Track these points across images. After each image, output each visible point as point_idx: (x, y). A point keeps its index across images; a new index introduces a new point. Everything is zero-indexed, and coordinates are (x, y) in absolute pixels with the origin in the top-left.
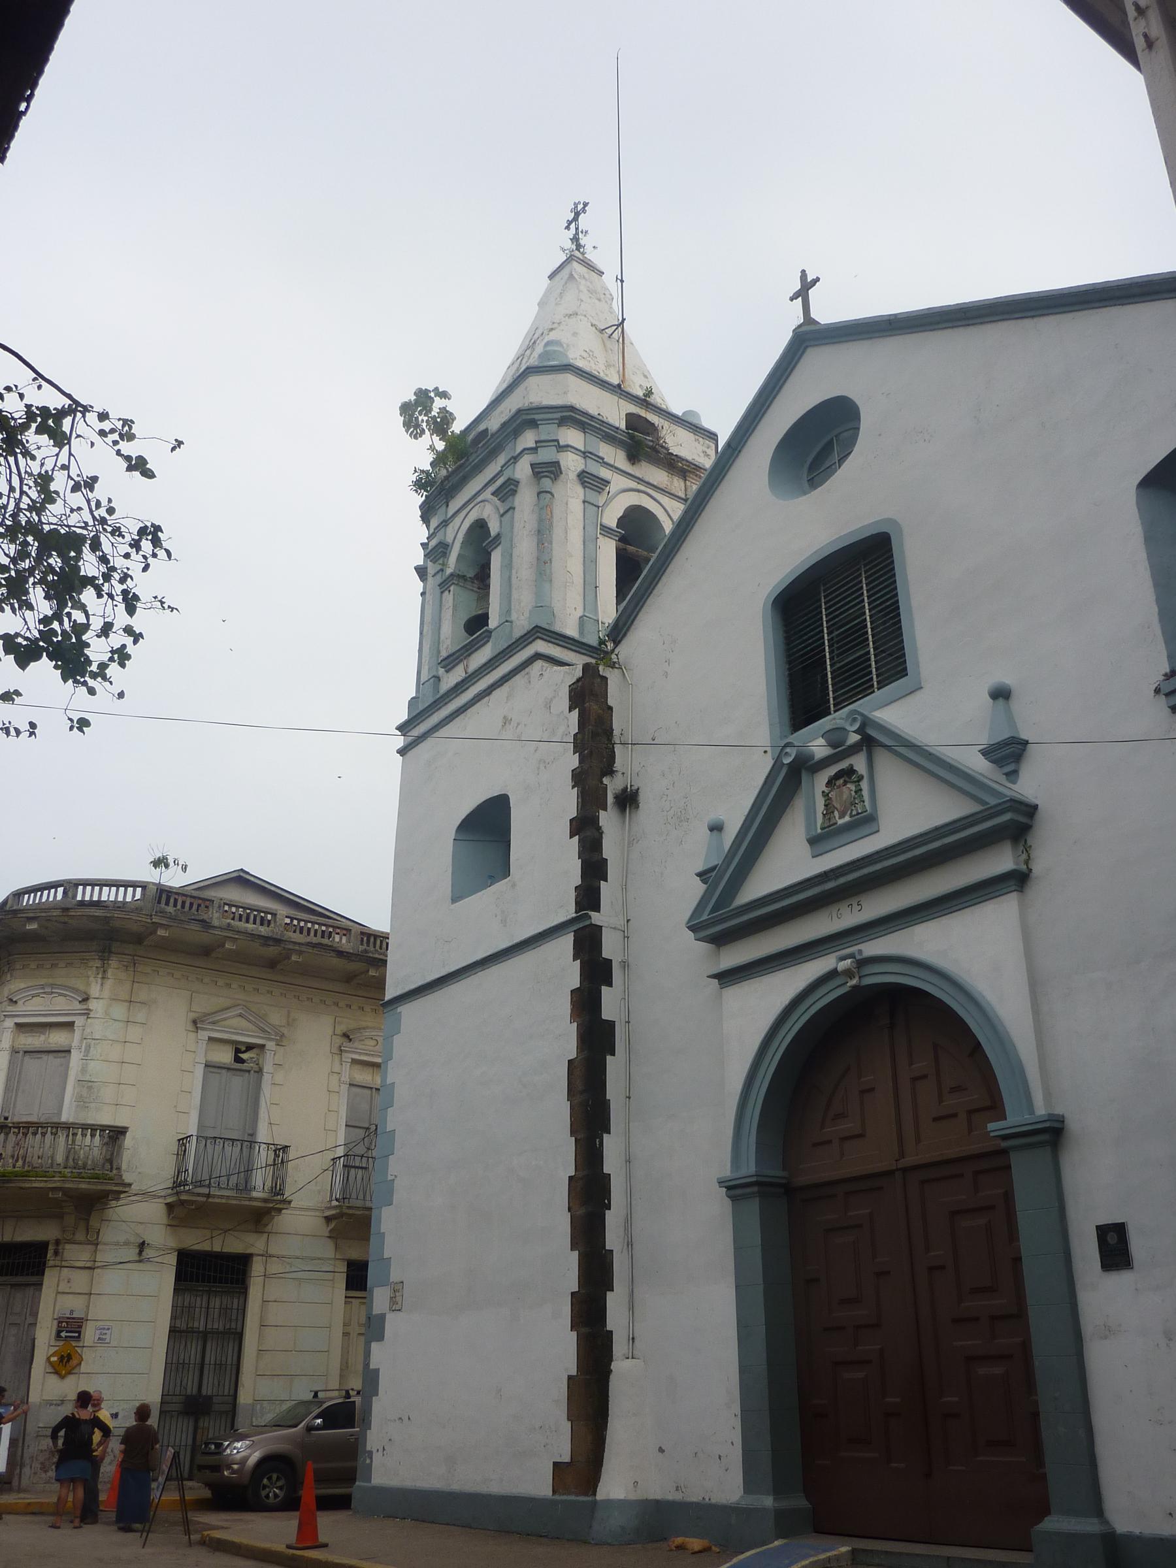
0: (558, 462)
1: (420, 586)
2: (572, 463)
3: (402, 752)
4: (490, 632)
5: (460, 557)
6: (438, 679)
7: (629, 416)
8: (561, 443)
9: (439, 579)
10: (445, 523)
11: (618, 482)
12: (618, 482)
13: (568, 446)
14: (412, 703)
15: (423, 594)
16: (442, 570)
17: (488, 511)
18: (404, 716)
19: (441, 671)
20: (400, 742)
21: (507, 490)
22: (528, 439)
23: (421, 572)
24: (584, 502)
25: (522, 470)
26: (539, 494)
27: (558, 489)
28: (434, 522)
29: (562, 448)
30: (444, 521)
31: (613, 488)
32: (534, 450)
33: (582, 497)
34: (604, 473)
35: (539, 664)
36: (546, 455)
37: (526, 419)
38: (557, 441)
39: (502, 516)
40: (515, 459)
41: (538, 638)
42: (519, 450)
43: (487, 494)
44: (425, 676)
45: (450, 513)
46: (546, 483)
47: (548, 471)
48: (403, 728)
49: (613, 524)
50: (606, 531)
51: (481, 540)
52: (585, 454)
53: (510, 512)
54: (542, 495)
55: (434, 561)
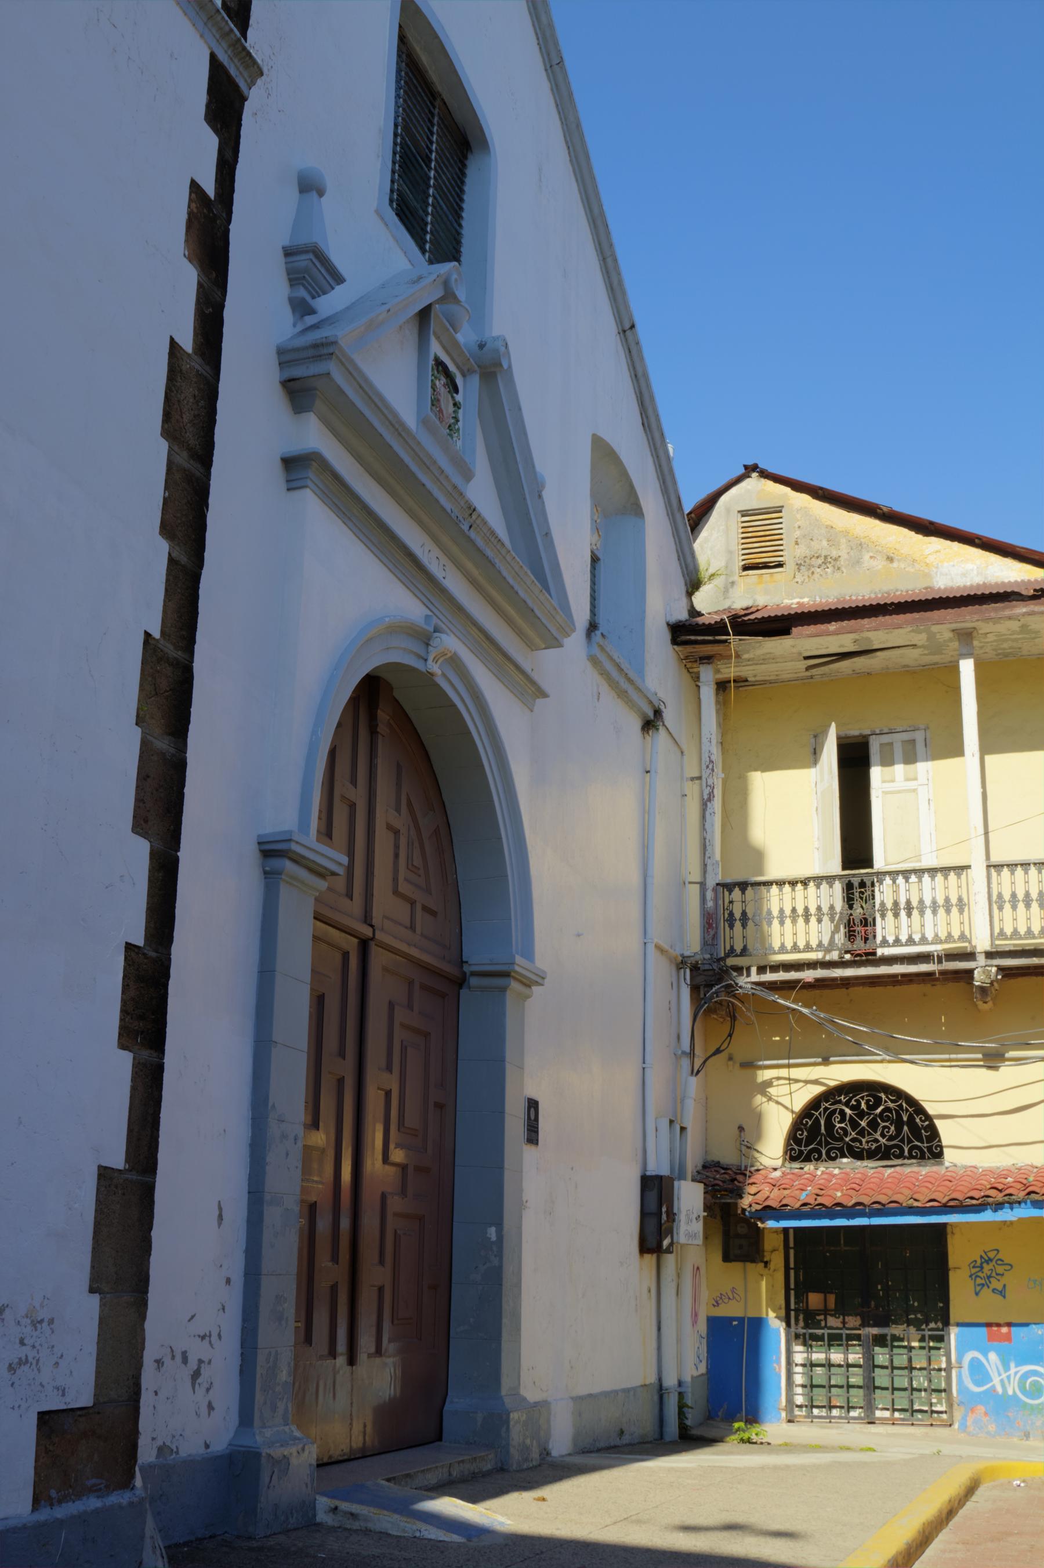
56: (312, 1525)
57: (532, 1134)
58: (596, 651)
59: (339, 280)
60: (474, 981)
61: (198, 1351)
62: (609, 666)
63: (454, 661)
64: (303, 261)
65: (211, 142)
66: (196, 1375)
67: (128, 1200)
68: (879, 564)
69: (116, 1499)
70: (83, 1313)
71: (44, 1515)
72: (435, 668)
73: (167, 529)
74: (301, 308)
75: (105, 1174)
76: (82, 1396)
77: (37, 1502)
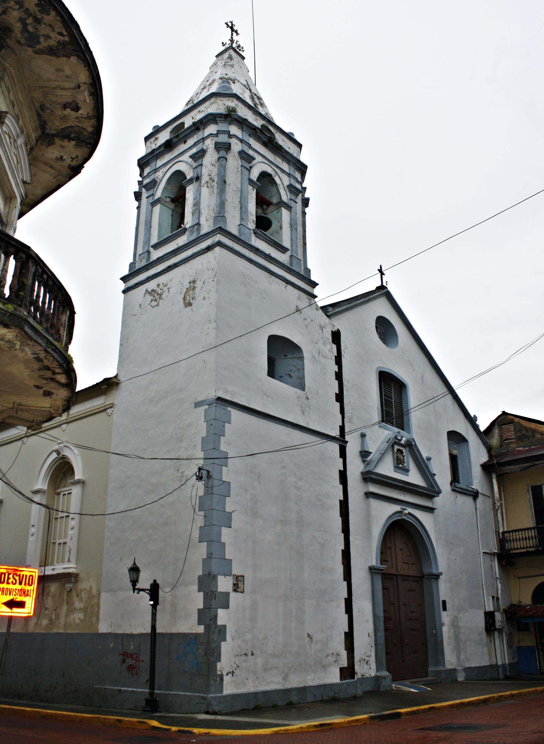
0: (230, 143)
1: (136, 204)
2: (236, 146)
3: (124, 292)
4: (186, 229)
5: (165, 189)
6: (149, 252)
7: (262, 126)
8: (231, 133)
9: (151, 200)
10: (156, 170)
11: (258, 158)
12: (258, 158)
13: (235, 136)
14: (132, 265)
15: (138, 208)
16: (153, 195)
17: (184, 165)
18: (126, 272)
19: (151, 249)
20: (122, 286)
21: (199, 156)
22: (212, 129)
23: (138, 196)
24: (242, 166)
25: (210, 144)
26: (219, 159)
27: (230, 157)
28: (147, 171)
29: (230, 136)
30: (156, 170)
31: (254, 162)
32: (216, 135)
33: (240, 165)
34: (251, 153)
35: (217, 249)
36: (223, 138)
37: (211, 118)
38: (229, 131)
39: (195, 168)
40: (203, 139)
41: (219, 233)
42: (206, 135)
43: (186, 157)
44: (140, 251)
45: (157, 166)
46: (222, 153)
47: (223, 148)
48: (124, 279)
49: (255, 179)
50: (251, 181)
51: (179, 182)
52: (241, 141)
53: (199, 168)
54: (221, 159)
55: (148, 190)
56: (392, 689)
57: (445, 609)
58: (453, 488)
59: (371, 453)
60: (425, 577)
61: (367, 659)
62: (458, 490)
63: (409, 514)
64: (363, 454)
65: (341, 460)
66: (367, 663)
67: (349, 637)
68: (539, 436)
69: (352, 680)
70: (344, 654)
71: (342, 682)
72: (404, 517)
73: (343, 532)
74: (364, 461)
75: (345, 633)
76: (346, 665)
77: (341, 680)
